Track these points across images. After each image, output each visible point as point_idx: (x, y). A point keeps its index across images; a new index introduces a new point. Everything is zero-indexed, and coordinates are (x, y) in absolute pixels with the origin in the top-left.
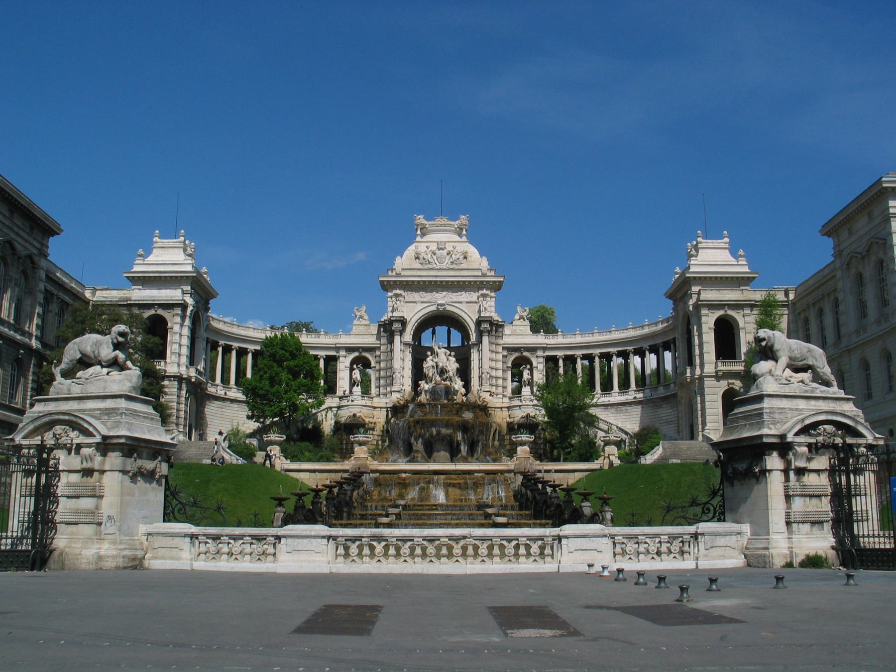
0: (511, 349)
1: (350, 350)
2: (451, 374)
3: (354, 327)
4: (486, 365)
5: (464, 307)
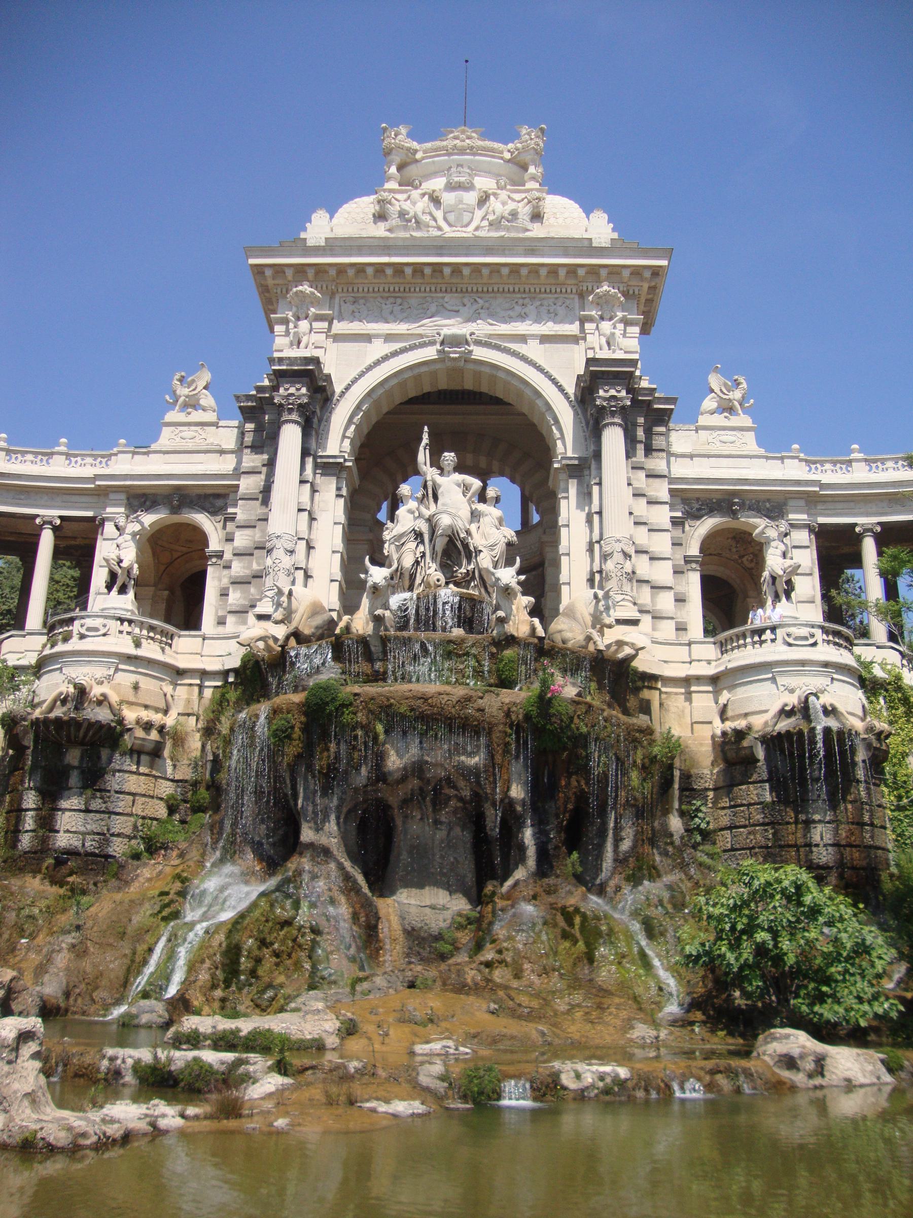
0: (692, 503)
1: (140, 498)
2: (485, 561)
3: (166, 431)
4: (618, 527)
5: (533, 350)
